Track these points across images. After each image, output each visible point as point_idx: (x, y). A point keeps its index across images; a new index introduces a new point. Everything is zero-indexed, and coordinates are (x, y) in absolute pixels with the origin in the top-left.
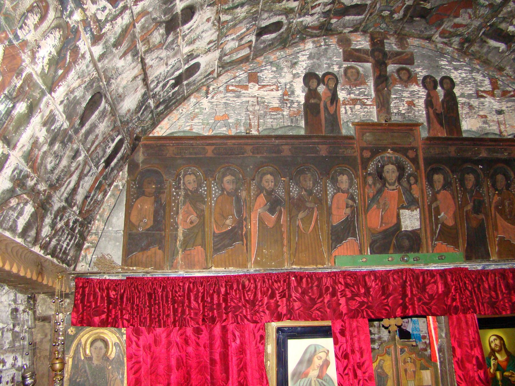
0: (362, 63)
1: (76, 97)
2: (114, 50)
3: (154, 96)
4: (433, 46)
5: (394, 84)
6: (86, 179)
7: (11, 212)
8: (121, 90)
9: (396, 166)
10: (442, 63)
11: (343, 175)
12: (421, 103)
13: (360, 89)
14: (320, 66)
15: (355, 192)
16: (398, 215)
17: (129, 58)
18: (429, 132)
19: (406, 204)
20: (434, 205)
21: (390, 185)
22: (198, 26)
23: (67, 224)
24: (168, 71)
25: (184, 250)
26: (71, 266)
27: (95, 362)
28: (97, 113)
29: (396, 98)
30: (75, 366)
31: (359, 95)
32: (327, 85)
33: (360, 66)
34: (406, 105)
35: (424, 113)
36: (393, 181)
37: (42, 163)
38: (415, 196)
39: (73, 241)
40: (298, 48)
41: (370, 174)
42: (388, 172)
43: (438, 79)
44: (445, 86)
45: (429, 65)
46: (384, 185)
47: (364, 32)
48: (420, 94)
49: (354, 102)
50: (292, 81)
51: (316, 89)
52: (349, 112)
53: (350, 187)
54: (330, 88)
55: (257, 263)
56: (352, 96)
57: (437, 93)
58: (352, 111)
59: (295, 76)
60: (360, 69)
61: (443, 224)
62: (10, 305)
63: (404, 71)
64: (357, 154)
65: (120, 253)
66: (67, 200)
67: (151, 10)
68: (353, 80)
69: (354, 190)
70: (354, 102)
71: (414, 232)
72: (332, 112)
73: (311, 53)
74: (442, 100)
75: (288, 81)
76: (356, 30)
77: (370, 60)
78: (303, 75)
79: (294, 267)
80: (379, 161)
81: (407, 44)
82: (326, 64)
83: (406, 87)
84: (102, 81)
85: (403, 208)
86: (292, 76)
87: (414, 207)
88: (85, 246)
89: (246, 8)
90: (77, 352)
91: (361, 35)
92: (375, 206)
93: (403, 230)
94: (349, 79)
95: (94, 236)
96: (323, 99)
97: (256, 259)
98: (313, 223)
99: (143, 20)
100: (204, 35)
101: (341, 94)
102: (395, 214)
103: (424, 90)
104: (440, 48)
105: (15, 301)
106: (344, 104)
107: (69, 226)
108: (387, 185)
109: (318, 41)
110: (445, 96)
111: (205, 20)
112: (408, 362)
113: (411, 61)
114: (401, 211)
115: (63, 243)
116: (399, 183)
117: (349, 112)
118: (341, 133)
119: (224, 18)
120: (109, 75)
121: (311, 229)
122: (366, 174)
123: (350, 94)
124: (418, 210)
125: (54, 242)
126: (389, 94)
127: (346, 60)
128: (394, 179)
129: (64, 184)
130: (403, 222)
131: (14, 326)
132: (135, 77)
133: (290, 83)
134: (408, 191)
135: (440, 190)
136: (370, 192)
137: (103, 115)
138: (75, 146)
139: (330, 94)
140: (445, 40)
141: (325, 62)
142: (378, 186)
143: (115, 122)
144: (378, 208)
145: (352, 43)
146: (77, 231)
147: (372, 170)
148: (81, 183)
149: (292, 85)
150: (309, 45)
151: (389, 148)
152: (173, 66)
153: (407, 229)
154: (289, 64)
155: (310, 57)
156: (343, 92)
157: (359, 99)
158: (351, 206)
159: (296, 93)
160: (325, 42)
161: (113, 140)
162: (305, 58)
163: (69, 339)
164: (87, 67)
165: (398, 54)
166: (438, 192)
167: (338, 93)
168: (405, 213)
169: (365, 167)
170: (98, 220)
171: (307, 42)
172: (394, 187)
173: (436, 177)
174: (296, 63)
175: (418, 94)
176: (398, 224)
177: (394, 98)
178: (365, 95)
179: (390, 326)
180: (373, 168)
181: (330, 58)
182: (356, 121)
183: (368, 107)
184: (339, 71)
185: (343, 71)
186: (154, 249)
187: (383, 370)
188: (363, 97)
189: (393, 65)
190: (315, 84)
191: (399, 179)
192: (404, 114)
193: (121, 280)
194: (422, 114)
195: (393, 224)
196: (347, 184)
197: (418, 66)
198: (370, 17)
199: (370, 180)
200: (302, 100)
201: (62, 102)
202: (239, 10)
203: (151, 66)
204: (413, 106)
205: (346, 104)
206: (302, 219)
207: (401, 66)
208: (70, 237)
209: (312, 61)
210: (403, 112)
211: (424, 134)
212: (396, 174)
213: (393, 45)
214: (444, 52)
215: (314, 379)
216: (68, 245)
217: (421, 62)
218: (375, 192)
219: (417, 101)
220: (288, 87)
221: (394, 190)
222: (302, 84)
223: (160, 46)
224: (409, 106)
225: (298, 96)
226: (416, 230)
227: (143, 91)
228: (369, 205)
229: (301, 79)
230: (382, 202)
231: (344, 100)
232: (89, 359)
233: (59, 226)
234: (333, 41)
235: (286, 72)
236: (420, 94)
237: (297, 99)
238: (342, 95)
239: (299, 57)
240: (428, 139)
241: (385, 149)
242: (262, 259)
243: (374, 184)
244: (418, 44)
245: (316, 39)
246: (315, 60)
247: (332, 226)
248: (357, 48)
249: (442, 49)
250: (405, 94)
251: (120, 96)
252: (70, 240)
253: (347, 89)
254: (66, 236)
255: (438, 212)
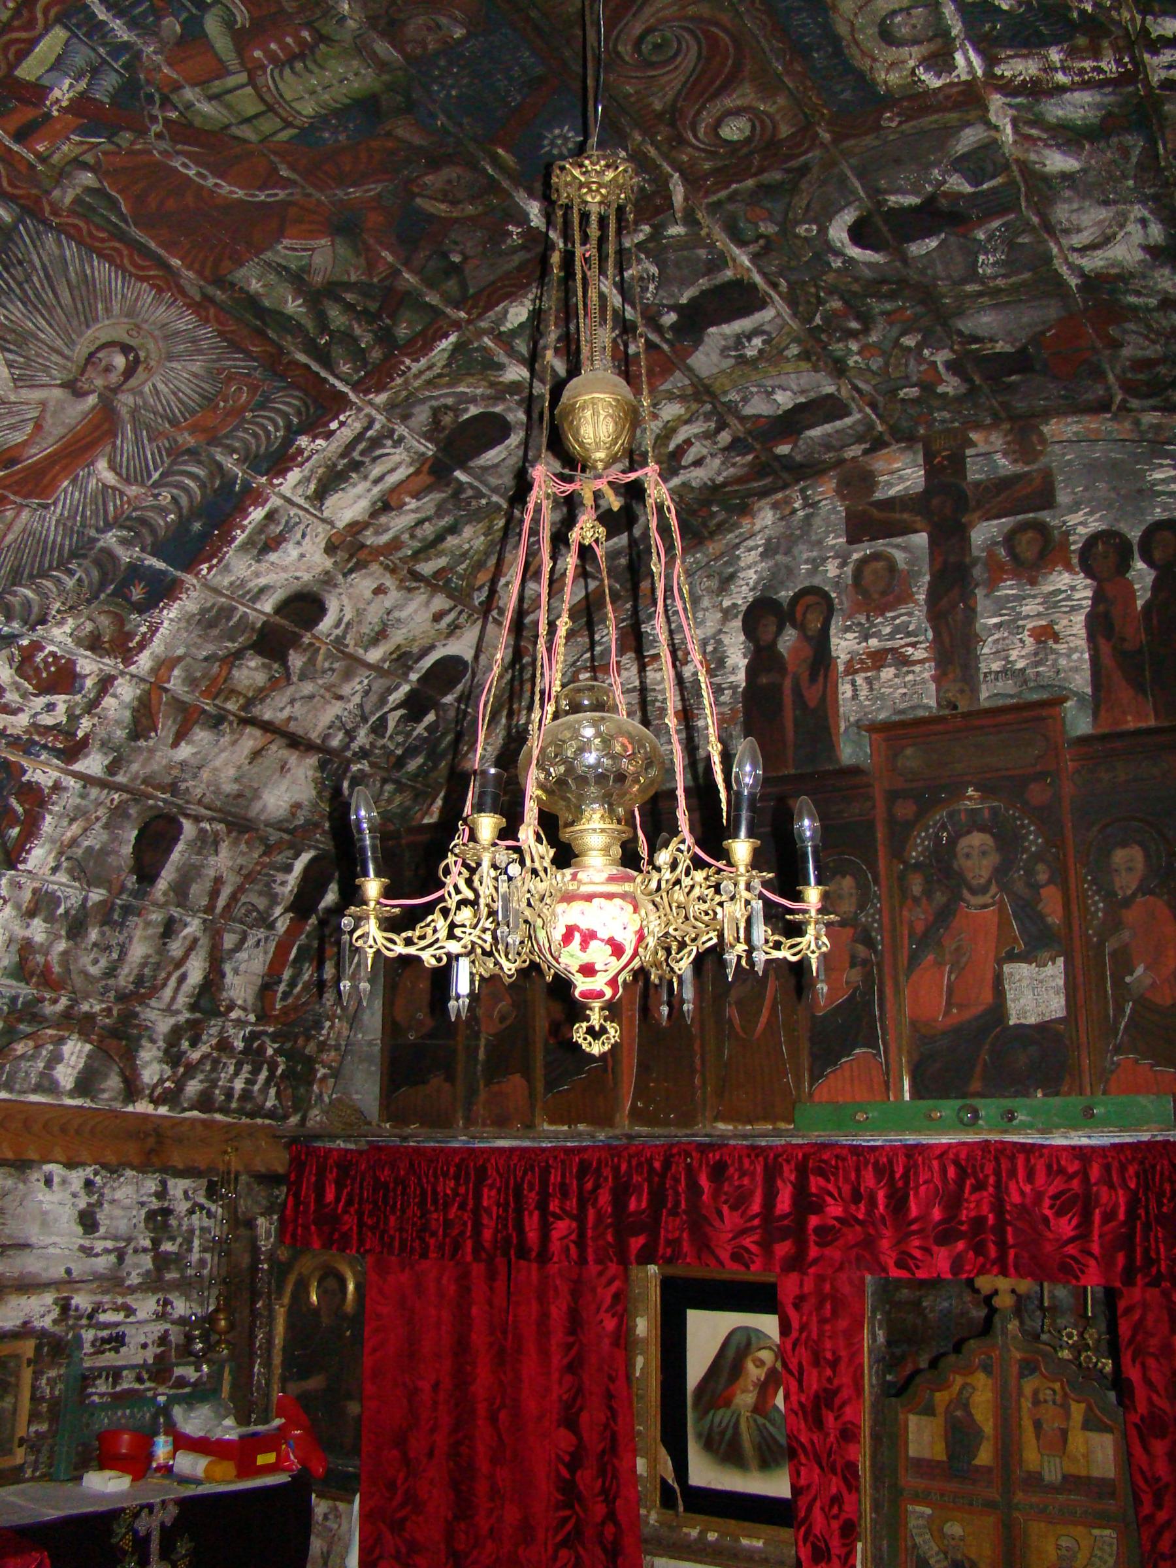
0: (906, 538)
1: (89, 849)
2: (142, 743)
3: (364, 754)
4: (1127, 425)
5: (992, 584)
6: (242, 955)
7: (24, 1065)
8: (229, 788)
9: (992, 835)
10: (1158, 476)
11: (844, 876)
12: (1075, 627)
13: (894, 618)
14: (790, 571)
15: (875, 921)
16: (998, 980)
17: (201, 735)
18: (1096, 715)
19: (1019, 948)
20: (1109, 947)
21: (973, 892)
22: (360, 613)
23: (224, 1045)
24: (360, 706)
25: (488, 1083)
26: (286, 1117)
27: (325, 1321)
28: (180, 847)
29: (998, 626)
30: (290, 1327)
31: (891, 636)
32: (801, 627)
33: (897, 546)
34: (1029, 641)
35: (1086, 656)
36: (982, 881)
37: (68, 971)
38: (1049, 920)
39: (264, 1074)
40: (737, 532)
41: (918, 866)
42: (968, 856)
43: (1134, 535)
44: (1157, 555)
45: (1113, 495)
46: (956, 898)
47: (907, 438)
48: (1077, 596)
49: (878, 659)
50: (720, 631)
51: (774, 643)
52: (864, 692)
53: (862, 907)
54: (810, 633)
55: (637, 1115)
56: (874, 642)
57: (1129, 584)
58: (871, 689)
59: (727, 614)
60: (899, 556)
61: (1142, 1003)
62: (142, 1204)
63: (1030, 534)
64: (880, 813)
65: (377, 1090)
66: (193, 1007)
67: (180, 651)
68: (876, 596)
69: (873, 916)
70: (878, 659)
71: (1043, 1028)
72: (812, 704)
73: (769, 540)
74: (1148, 605)
75: (710, 632)
76: (878, 444)
77: (918, 526)
78: (744, 608)
79: (721, 1126)
80: (943, 827)
81: (1043, 440)
82: (806, 562)
83: (1033, 582)
84: (150, 796)
85: (1012, 957)
86: (720, 615)
87: (1046, 955)
88: (319, 1075)
89: (468, 531)
90: (295, 1297)
91: (903, 450)
92: (931, 957)
93: (1011, 1023)
94: (865, 593)
95: (333, 1053)
96: (791, 667)
97: (634, 1106)
98: (765, 1013)
99: (176, 672)
100: (396, 614)
101: (843, 643)
102: (989, 976)
103: (1089, 581)
104: (1151, 426)
105: (161, 1194)
106: (850, 670)
107: (233, 1048)
108: (966, 894)
109: (788, 501)
110: (1156, 586)
111: (368, 594)
112: (1046, 1401)
113: (1045, 498)
114: (1007, 968)
115: (231, 1080)
116: (1003, 888)
117: (864, 692)
118: (838, 760)
119: (427, 568)
120: (168, 780)
121: (760, 1028)
122: (905, 869)
123: (866, 637)
124: (1060, 961)
125: (193, 1087)
126: (971, 614)
127: (853, 539)
128: (986, 874)
129: (164, 985)
130: (1014, 1001)
131: (156, 1243)
132: (256, 754)
133: (714, 637)
134: (1028, 910)
135: (1134, 895)
136: (919, 916)
137: (207, 843)
138: (156, 916)
139: (808, 652)
140: (1151, 402)
141: (805, 556)
142: (940, 898)
143: (264, 840)
144: (939, 964)
145: (878, 483)
146: (270, 1052)
147: (922, 853)
148: (227, 968)
149: (719, 642)
150: (766, 518)
151: (970, 784)
152: (367, 693)
153: (1023, 1021)
154: (714, 584)
155: (769, 551)
156: (849, 636)
157: (892, 649)
158: (865, 962)
159: (729, 662)
160: (805, 498)
161: (288, 869)
162: (754, 556)
163: (281, 1270)
164: (83, 796)
165: (1005, 484)
166: (1127, 902)
167: (834, 641)
168: (1020, 973)
169: (898, 852)
170: (340, 1018)
171: (760, 509)
172: (986, 899)
173: (1120, 856)
174: (732, 577)
175: (1069, 598)
176: (999, 1008)
177: (995, 625)
178: (909, 634)
179: (1013, 1291)
180: (926, 848)
181: (820, 542)
182: (882, 716)
183: (917, 668)
184: (838, 576)
185: (850, 573)
186: (436, 1081)
187: (970, 1415)
188: (902, 642)
189: (995, 522)
190: (773, 629)
191: (1000, 873)
192: (1023, 670)
193: (360, 1152)
194: (1080, 659)
195: (981, 1008)
196: (854, 900)
197: (1074, 508)
198: (881, 411)
199: (916, 886)
200: (740, 678)
201: (54, 870)
202: (451, 541)
203: (290, 718)
204: (1050, 642)
205: (856, 672)
206: (739, 1003)
207: (1020, 517)
208: (247, 1068)
209: (771, 563)
210: (1020, 665)
211: (1080, 723)
212: (994, 859)
213: (998, 456)
214: (1161, 438)
215: (745, 1414)
216: (250, 1082)
217: (1086, 489)
218: (931, 918)
219: (1065, 622)
220: (709, 649)
221: (985, 906)
222: (742, 638)
223: (274, 685)
224: (1038, 642)
225: (734, 671)
226: (1051, 1021)
227: (313, 760)
228: (914, 959)
229: (737, 623)
230: (950, 945)
231: (851, 660)
232: (316, 1312)
233: (195, 1056)
234: (825, 490)
235: (706, 609)
236: (1077, 596)
237: (732, 678)
238: (843, 645)
239: (738, 557)
240: (1083, 740)
241: (957, 791)
242: (647, 1106)
243: (928, 893)
244: (1075, 433)
245: (780, 495)
246: (778, 557)
247: (813, 1016)
248: (892, 492)
249: (1158, 428)
250: (1030, 607)
251: (240, 795)
252: (256, 1072)
253: (860, 624)
254: (231, 1069)
255: (1124, 963)
